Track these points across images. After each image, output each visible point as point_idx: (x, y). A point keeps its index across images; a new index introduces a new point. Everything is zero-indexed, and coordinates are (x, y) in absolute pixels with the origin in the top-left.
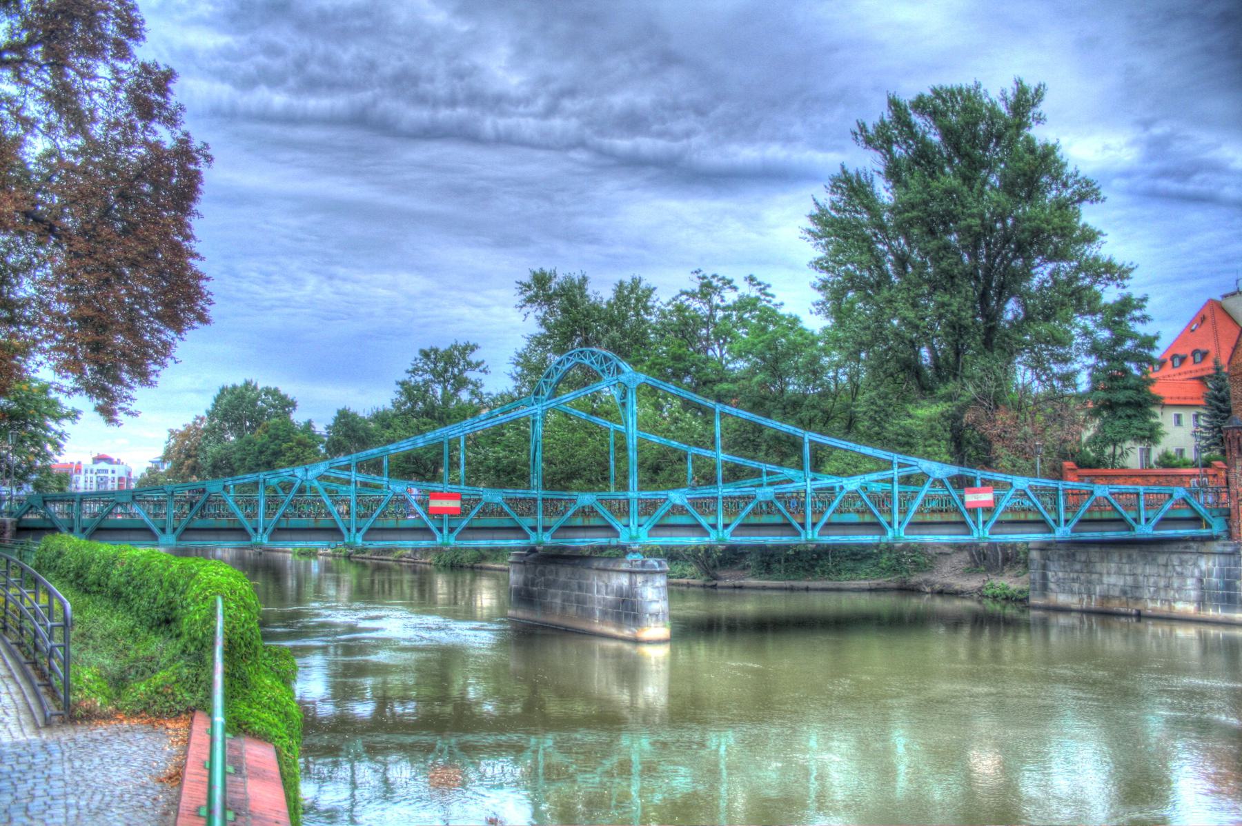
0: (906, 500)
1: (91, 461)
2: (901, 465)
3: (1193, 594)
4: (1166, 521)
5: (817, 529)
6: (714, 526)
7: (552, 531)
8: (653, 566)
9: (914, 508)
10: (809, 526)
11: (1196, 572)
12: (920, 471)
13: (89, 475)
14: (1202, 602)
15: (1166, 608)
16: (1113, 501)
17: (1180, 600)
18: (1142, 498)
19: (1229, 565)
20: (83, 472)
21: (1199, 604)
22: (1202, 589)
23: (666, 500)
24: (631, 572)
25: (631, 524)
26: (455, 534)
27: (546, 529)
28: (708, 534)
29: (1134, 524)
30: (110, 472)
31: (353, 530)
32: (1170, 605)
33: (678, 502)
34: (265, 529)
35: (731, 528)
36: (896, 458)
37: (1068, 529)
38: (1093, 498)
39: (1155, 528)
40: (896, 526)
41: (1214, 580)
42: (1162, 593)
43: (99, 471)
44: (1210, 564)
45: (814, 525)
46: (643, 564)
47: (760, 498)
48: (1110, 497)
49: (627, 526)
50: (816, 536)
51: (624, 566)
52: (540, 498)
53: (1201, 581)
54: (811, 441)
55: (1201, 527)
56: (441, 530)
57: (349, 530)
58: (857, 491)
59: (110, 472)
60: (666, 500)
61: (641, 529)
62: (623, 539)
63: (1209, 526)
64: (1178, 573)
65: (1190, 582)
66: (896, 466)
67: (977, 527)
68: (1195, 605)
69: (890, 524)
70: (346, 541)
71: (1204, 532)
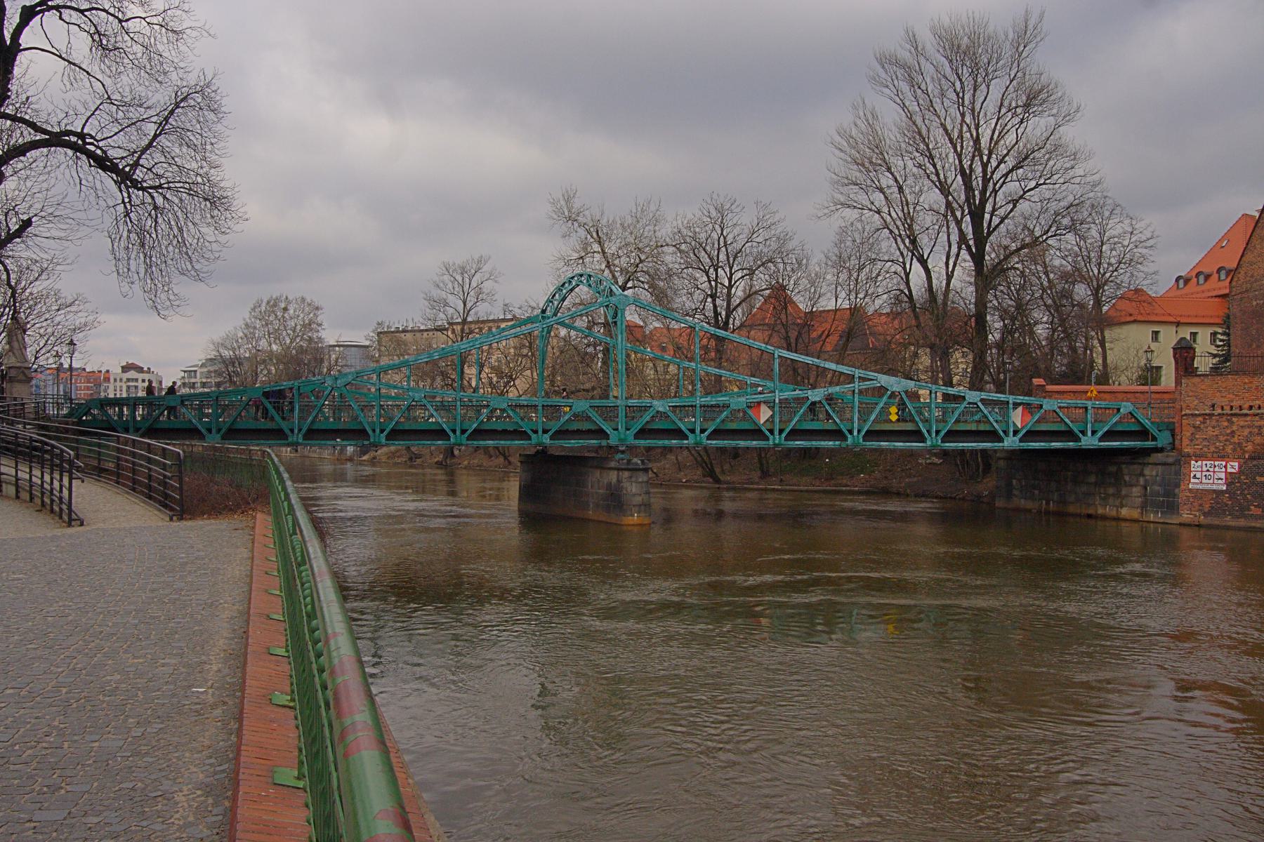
0: (865, 413)
1: (120, 370)
2: (862, 379)
4: (1110, 435)
5: (784, 435)
6: (693, 431)
7: (550, 433)
8: (637, 464)
9: (873, 417)
10: (776, 432)
12: (879, 385)
13: (118, 384)
16: (1061, 414)
18: (1090, 412)
20: (112, 380)
23: (651, 407)
24: (618, 469)
25: (620, 427)
26: (466, 435)
27: (545, 431)
28: (686, 438)
29: (1081, 435)
30: (140, 381)
31: (378, 431)
33: (661, 409)
34: (300, 430)
35: (707, 433)
36: (858, 373)
37: (1017, 439)
38: (1042, 411)
39: (1101, 440)
40: (855, 433)
43: (128, 380)
45: (781, 431)
46: (629, 462)
47: (733, 406)
48: (1058, 410)
49: (617, 429)
50: (783, 442)
51: (613, 464)
52: (540, 405)
54: (780, 356)
55: (1148, 440)
56: (454, 431)
57: (374, 431)
58: (820, 402)
59: (140, 381)
60: (651, 407)
61: (628, 432)
62: (613, 441)
63: (1154, 439)
66: (856, 380)
67: (930, 436)
69: (851, 432)
70: (372, 440)
71: (1149, 444)
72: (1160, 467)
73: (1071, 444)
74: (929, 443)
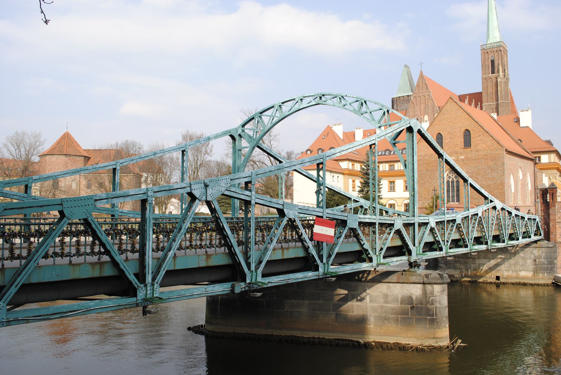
3: (531, 267)
11: (533, 256)
14: (536, 271)
15: (515, 274)
17: (523, 270)
19: (551, 253)
21: (534, 272)
22: (536, 264)
32: (517, 273)
41: (543, 260)
42: (513, 267)
44: (540, 252)
53: (535, 260)
64: (522, 257)
65: (529, 262)
68: (532, 272)
72: (544, 248)
73: (310, 275)
74: (321, 270)
